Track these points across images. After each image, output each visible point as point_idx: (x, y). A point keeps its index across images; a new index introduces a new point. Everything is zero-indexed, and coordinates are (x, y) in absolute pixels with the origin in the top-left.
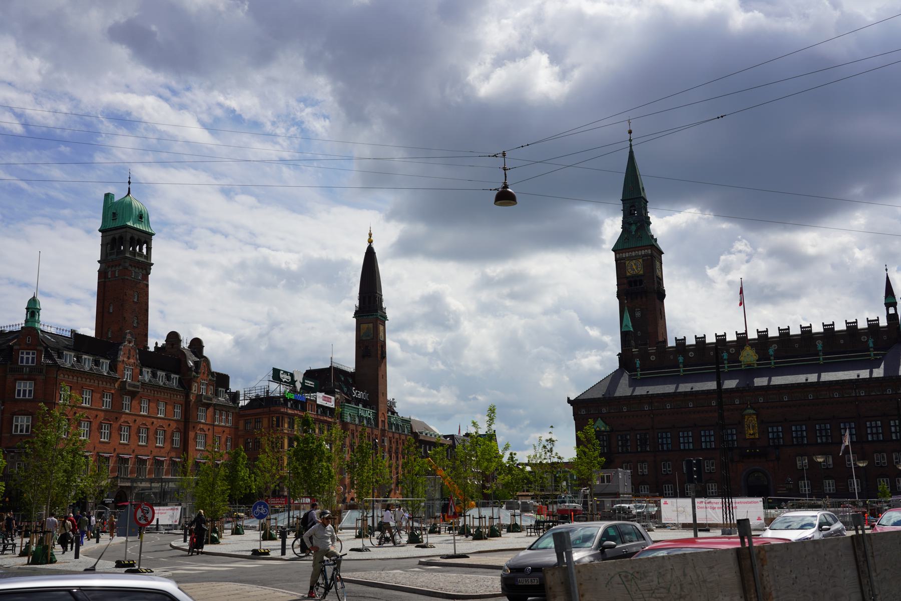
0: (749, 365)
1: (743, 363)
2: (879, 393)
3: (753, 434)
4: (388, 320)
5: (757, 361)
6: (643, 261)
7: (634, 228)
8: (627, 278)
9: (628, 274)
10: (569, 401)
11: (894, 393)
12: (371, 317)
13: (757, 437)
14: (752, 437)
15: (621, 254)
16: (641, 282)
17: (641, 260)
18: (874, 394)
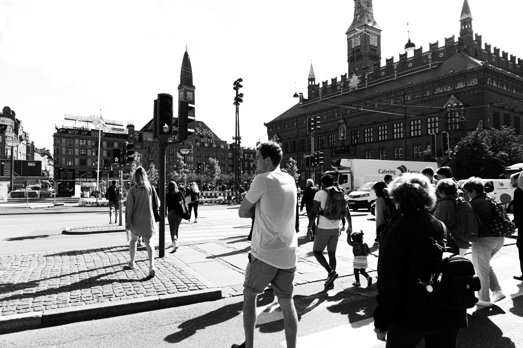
0: (354, 89)
1: (350, 88)
2: (420, 96)
3: (343, 137)
5: (359, 84)
6: (361, 37)
7: (359, 16)
8: (352, 49)
9: (353, 47)
10: (265, 124)
11: (431, 94)
12: (183, 88)
13: (345, 139)
14: (342, 139)
15: (350, 35)
16: (359, 50)
17: (359, 37)
18: (417, 97)
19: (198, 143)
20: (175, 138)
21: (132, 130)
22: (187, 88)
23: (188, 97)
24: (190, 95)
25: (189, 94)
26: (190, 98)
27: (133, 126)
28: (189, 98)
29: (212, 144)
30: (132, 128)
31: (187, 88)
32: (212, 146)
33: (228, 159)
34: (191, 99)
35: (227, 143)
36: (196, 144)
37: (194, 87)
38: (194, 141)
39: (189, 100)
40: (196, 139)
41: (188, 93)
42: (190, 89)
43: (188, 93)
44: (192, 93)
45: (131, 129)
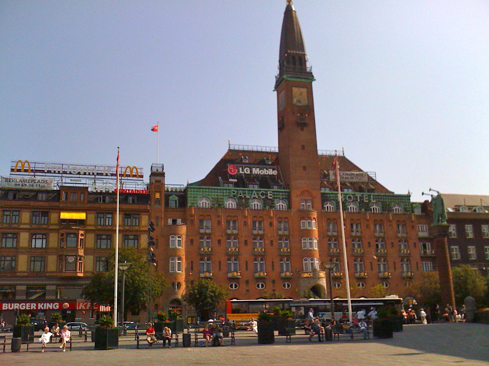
4: (315, 80)
12: (283, 82)
19: (329, 205)
20: (267, 195)
21: (160, 181)
22: (293, 79)
23: (295, 101)
24: (301, 94)
25: (298, 93)
26: (302, 100)
27: (163, 175)
28: (299, 101)
29: (367, 204)
30: (158, 178)
31: (293, 79)
32: (368, 209)
33: (417, 241)
34: (304, 102)
35: (413, 200)
36: (323, 208)
37: (310, 77)
38: (318, 200)
39: (299, 104)
40: (323, 194)
41: (295, 90)
42: (299, 80)
43: (295, 90)
44: (304, 90)
45: (156, 181)
